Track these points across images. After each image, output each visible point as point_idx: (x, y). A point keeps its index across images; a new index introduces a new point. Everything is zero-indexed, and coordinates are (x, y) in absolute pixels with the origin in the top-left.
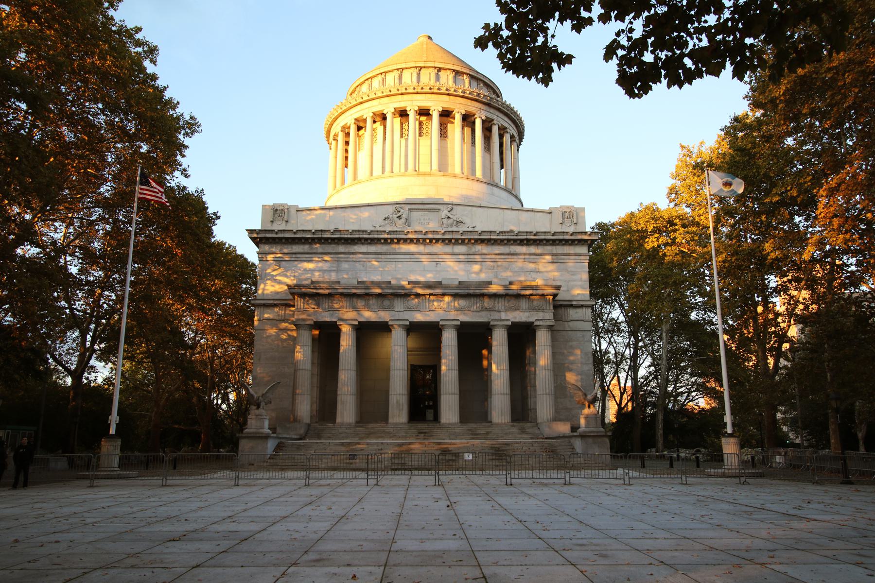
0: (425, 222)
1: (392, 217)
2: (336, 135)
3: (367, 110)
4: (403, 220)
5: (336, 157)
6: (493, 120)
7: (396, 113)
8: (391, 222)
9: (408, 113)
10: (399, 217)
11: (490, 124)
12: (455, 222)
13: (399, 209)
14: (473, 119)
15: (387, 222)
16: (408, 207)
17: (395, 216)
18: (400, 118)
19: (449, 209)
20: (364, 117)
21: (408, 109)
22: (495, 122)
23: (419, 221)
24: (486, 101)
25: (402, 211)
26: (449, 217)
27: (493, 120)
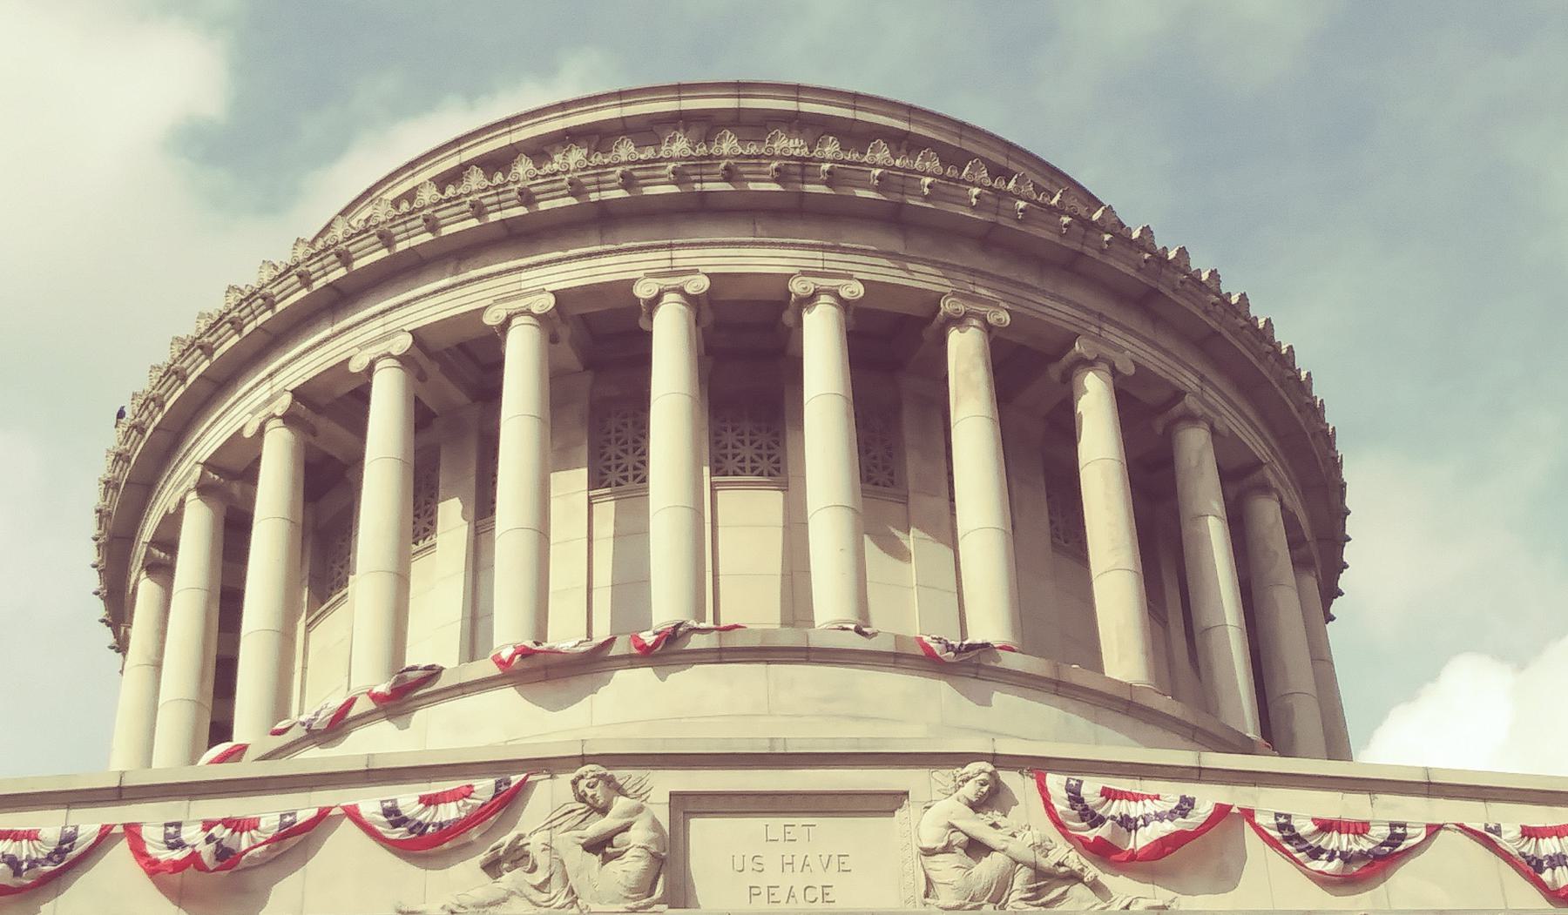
0: (798, 880)
1: (548, 847)
2: (167, 541)
3: (374, 329)
4: (631, 866)
5: (158, 666)
6: (1179, 395)
7: (565, 332)
8: (539, 877)
9: (643, 323)
10: (601, 847)
11: (1159, 425)
12: (1022, 875)
13: (599, 792)
14: (1054, 372)
15: (510, 879)
16: (663, 784)
17: (569, 845)
18: (588, 377)
19: (970, 790)
20: (356, 366)
21: (643, 291)
22: (1190, 402)
23: (750, 878)
24: (1131, 272)
25: (620, 804)
26: (976, 848)
27: (1179, 395)
